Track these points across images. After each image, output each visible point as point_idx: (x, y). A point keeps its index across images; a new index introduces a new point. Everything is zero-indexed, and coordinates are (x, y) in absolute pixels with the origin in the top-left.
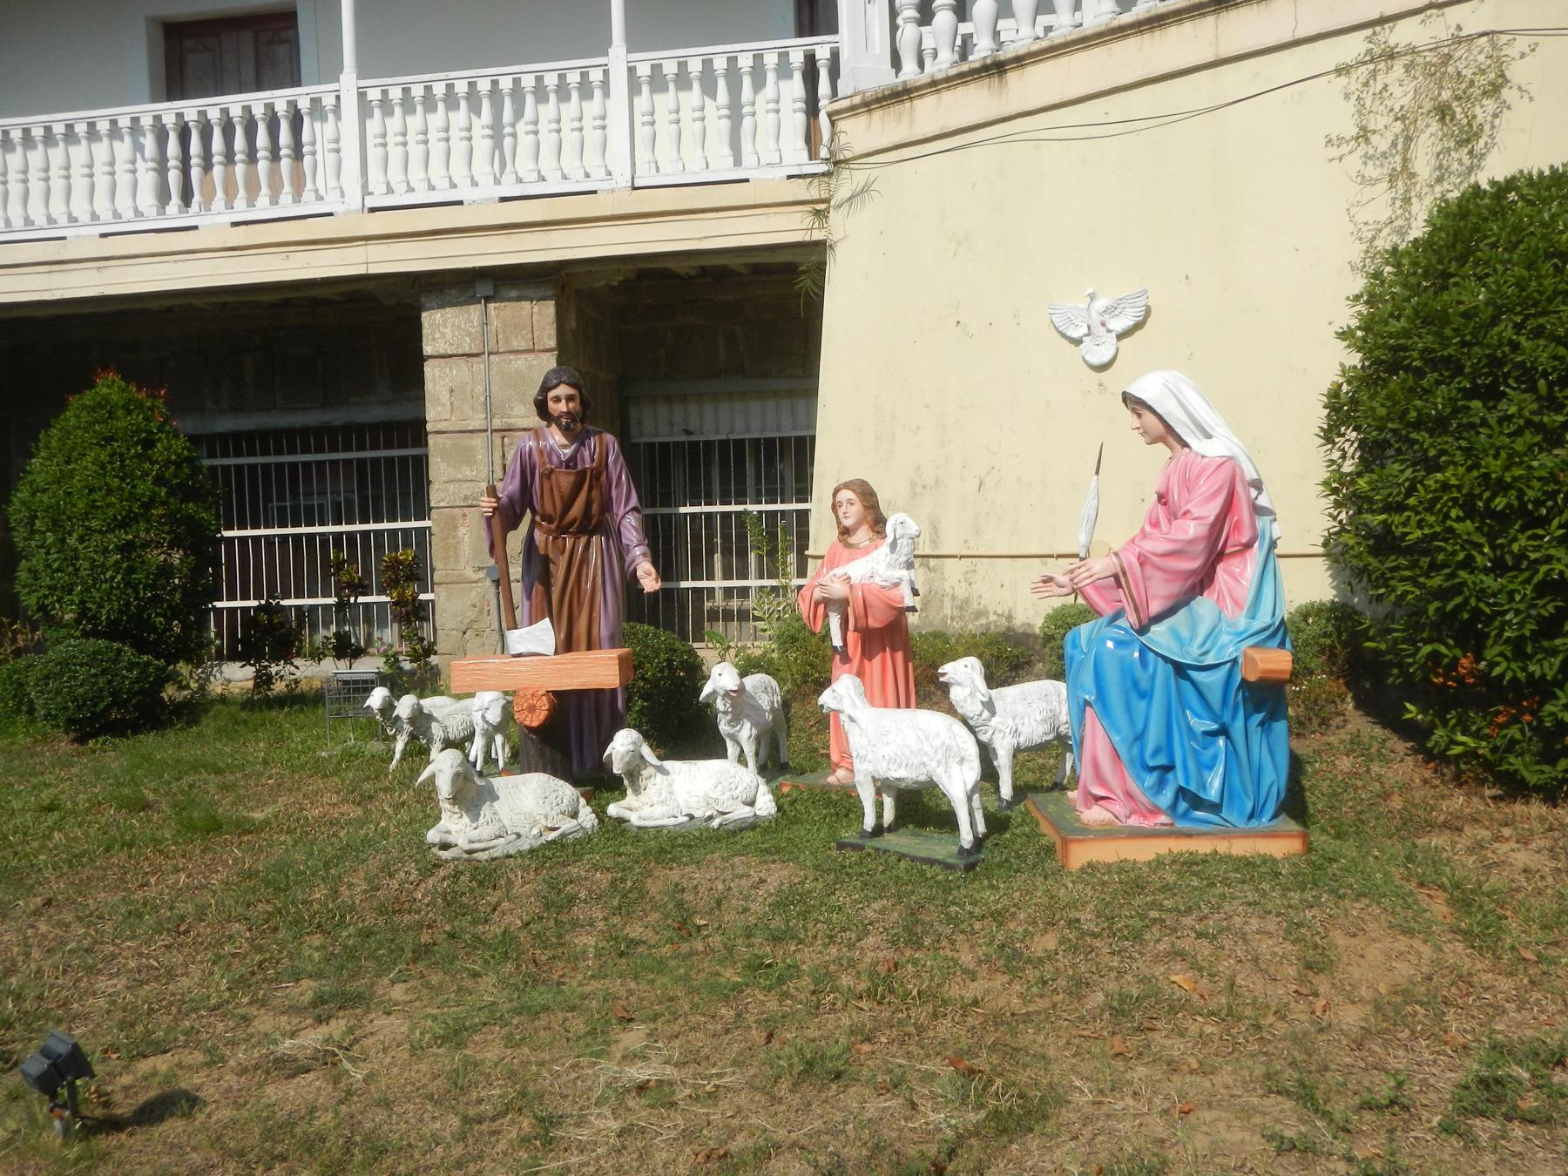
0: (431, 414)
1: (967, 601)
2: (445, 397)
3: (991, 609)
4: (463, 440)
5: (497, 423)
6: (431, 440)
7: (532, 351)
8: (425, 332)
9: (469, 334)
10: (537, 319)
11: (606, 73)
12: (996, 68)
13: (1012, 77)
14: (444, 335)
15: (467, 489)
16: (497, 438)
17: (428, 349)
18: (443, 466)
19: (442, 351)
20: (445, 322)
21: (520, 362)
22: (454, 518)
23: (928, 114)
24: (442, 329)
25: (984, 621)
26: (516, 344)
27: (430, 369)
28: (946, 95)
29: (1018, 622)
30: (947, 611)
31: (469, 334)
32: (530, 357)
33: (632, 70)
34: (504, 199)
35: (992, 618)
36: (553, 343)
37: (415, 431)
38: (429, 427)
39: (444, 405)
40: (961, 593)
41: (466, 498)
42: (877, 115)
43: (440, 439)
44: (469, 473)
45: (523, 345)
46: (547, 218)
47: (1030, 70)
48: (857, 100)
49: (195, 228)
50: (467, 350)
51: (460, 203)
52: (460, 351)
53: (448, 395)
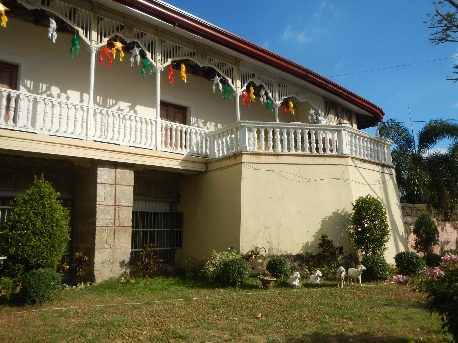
1: (278, 249)
2: (103, 195)
3: (283, 250)
4: (107, 208)
5: (117, 204)
7: (127, 185)
8: (98, 176)
9: (111, 179)
11: (156, 122)
12: (278, 155)
13: (280, 157)
14: (104, 178)
15: (107, 222)
17: (99, 181)
18: (101, 214)
19: (103, 182)
20: (104, 174)
21: (124, 188)
22: (103, 229)
23: (263, 159)
24: (104, 175)
25: (282, 253)
26: (123, 183)
27: (99, 187)
28: (267, 156)
29: (289, 253)
30: (274, 251)
31: (111, 179)
33: (162, 124)
34: (130, 146)
35: (283, 252)
36: (133, 184)
38: (97, 203)
40: (277, 248)
42: (252, 156)
43: (101, 207)
44: (108, 217)
45: (125, 184)
47: (283, 157)
48: (249, 152)
49: (36, 133)
50: (110, 183)
51: (119, 145)
53: (103, 194)
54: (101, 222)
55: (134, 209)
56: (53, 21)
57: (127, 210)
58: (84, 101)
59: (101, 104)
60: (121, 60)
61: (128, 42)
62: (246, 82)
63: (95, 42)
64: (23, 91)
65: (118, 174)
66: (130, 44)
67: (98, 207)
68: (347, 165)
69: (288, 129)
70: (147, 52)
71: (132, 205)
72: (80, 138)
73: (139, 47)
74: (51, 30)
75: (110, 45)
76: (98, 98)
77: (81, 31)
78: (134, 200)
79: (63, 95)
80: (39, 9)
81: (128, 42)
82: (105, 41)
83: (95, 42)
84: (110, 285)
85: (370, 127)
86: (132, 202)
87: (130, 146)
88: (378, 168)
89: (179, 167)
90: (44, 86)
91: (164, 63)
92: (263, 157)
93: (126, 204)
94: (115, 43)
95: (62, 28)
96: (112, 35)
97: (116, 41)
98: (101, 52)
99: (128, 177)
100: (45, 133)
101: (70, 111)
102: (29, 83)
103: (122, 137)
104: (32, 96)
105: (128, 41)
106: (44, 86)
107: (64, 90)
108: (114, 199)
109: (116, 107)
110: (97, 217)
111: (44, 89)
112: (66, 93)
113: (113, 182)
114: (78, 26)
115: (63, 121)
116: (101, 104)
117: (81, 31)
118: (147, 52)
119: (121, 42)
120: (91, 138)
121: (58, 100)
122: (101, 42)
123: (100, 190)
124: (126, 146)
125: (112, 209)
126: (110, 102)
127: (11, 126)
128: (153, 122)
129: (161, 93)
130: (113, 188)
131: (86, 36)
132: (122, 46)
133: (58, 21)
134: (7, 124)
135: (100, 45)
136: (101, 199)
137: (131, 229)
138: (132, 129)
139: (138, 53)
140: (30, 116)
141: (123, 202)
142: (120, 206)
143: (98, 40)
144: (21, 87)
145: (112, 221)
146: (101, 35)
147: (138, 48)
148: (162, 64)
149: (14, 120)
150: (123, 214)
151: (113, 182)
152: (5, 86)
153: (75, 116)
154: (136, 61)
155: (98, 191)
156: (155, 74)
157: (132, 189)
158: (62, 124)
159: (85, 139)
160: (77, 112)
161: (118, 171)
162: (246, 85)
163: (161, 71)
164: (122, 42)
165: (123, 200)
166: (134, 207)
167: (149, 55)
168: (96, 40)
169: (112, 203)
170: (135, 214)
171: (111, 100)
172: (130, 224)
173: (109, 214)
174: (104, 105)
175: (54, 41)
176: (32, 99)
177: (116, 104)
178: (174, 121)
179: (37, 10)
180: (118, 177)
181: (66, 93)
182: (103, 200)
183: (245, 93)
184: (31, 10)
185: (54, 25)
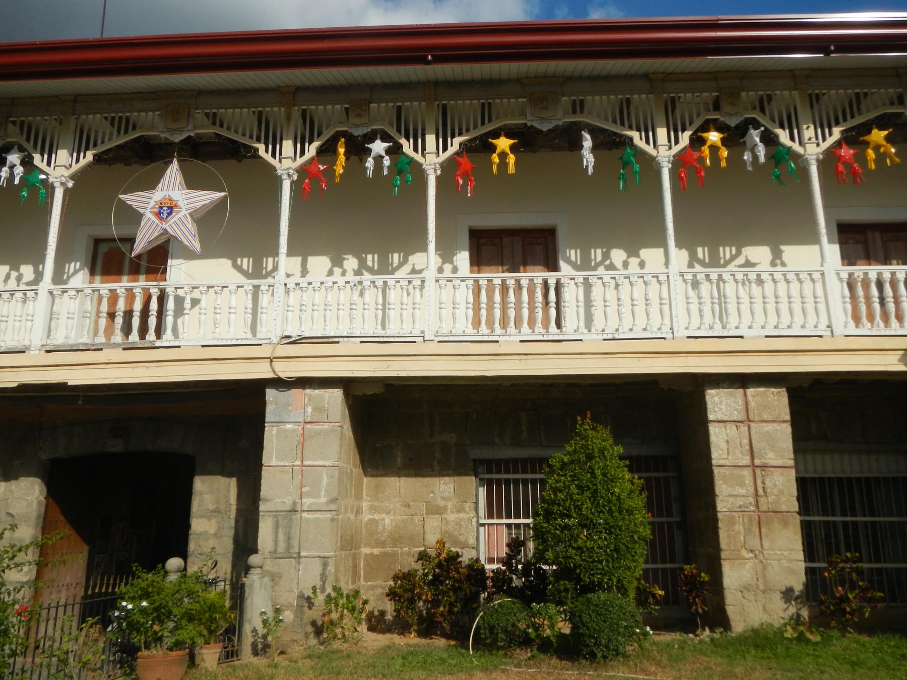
2: (724, 445)
4: (736, 471)
5: (757, 462)
9: (736, 410)
14: (720, 409)
17: (711, 417)
18: (724, 486)
19: (720, 419)
20: (721, 402)
21: (769, 427)
22: (733, 518)
24: (720, 404)
27: (713, 429)
31: (736, 410)
32: (774, 425)
34: (767, 337)
36: (788, 418)
38: (714, 462)
39: (722, 450)
41: (740, 506)
43: (722, 470)
45: (770, 418)
46: (797, 348)
50: (735, 418)
51: (742, 337)
52: (731, 419)
53: (724, 444)
54: (727, 502)
55: (797, 472)
56: (588, 136)
57: (782, 474)
58: (308, 272)
59: (707, 261)
60: (723, 164)
61: (733, 125)
63: (664, 148)
64: (565, 269)
65: (750, 398)
66: (737, 127)
67: (716, 471)
70: (779, 131)
71: (792, 463)
72: (491, 339)
73: (757, 125)
75: (697, 141)
76: (700, 250)
77: (261, 147)
78: (796, 451)
79: (634, 261)
81: (733, 125)
82: (685, 138)
83: (664, 148)
84: (761, 641)
86: (792, 456)
87: (767, 337)
90: (599, 251)
91: (824, 139)
93: (779, 462)
94: (704, 135)
95: (608, 143)
96: (698, 123)
97: (708, 131)
98: (680, 161)
99: (777, 400)
100: (595, 337)
101: (635, 288)
103: (746, 319)
104: (580, 275)
105: (733, 122)
106: (599, 251)
107: (633, 252)
109: (407, 268)
110: (718, 490)
112: (638, 256)
113: (741, 416)
114: (631, 128)
115: (623, 311)
116: (707, 261)
117: (635, 135)
118: (779, 131)
119: (719, 129)
120: (681, 333)
121: (626, 272)
122: (677, 142)
123: (718, 436)
124: (758, 337)
125: (747, 473)
126: (726, 252)
127: (540, 334)
128: (816, 276)
129: (826, 207)
130: (744, 429)
131: (648, 142)
132: (721, 136)
133: (595, 132)
134: (533, 332)
135: (676, 149)
136: (720, 455)
137: (798, 517)
138: (792, 300)
139: (758, 139)
140: (582, 311)
141: (771, 458)
142: (764, 467)
143: (669, 141)
144: (562, 264)
145: (751, 500)
146: (675, 129)
147: (756, 129)
148: (818, 145)
149: (559, 325)
150: (775, 485)
151: (741, 416)
152: (540, 267)
153: (646, 295)
154: (755, 157)
155: (713, 438)
156: (804, 172)
157: (787, 429)
158: (623, 316)
159: (670, 336)
160: (649, 287)
161: (751, 391)
163: (818, 160)
164: (720, 127)
165: (771, 455)
166: (797, 467)
167: (783, 136)
168: (666, 143)
169: (746, 460)
170: (803, 483)
171: (727, 249)
172: (795, 506)
173: (742, 485)
174: (715, 261)
175: (590, 170)
177: (739, 253)
178: (886, 261)
179: (190, 137)
180: (752, 404)
181: (638, 256)
182: (725, 456)
184: (549, 130)
185: (588, 143)
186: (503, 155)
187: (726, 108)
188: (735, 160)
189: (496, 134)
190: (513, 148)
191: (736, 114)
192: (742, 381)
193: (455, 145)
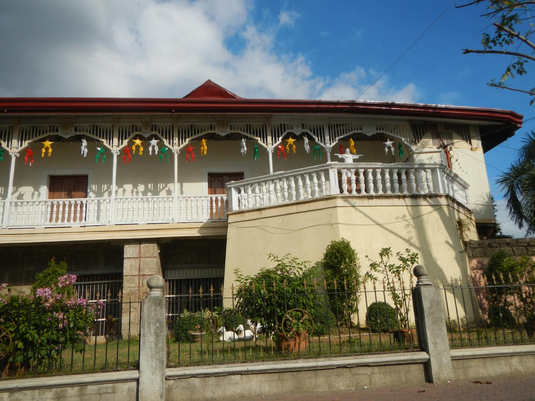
0: (124, 272)
2: (129, 267)
4: (132, 278)
5: (141, 273)
6: (124, 277)
7: (150, 257)
10: (154, 249)
13: (263, 211)
16: (141, 277)
17: (125, 256)
21: (147, 260)
24: (129, 251)
26: (147, 256)
27: (125, 261)
37: (120, 276)
42: (237, 215)
44: (134, 285)
45: (149, 256)
47: (266, 210)
53: (129, 267)
60: (141, 153)
62: (282, 134)
65: (142, 248)
68: (335, 207)
69: (374, 169)
70: (164, 140)
74: (83, 148)
75: (131, 143)
79: (121, 190)
80: (74, 135)
82: (125, 142)
85: (508, 139)
88: (408, 201)
89: (199, 235)
90: (106, 186)
92: (246, 215)
94: (134, 141)
96: (132, 136)
97: (136, 139)
102: (94, 187)
106: (106, 186)
108: (141, 269)
110: (124, 286)
111: (105, 189)
112: (123, 187)
119: (140, 139)
122: (122, 144)
123: (127, 263)
125: (136, 278)
126: (161, 186)
131: (110, 144)
142: (144, 275)
145: (137, 288)
155: (125, 265)
161: (142, 245)
162: (280, 138)
165: (147, 270)
167: (166, 142)
169: (137, 273)
171: (161, 184)
173: (134, 283)
175: (85, 155)
176: (49, 203)
177: (166, 186)
181: (123, 187)
183: (280, 147)
184: (69, 138)
186: (47, 149)
187: (143, 130)
188: (146, 150)
189: (44, 140)
190: (52, 146)
191: (147, 133)
192: (139, 241)
193: (26, 144)
